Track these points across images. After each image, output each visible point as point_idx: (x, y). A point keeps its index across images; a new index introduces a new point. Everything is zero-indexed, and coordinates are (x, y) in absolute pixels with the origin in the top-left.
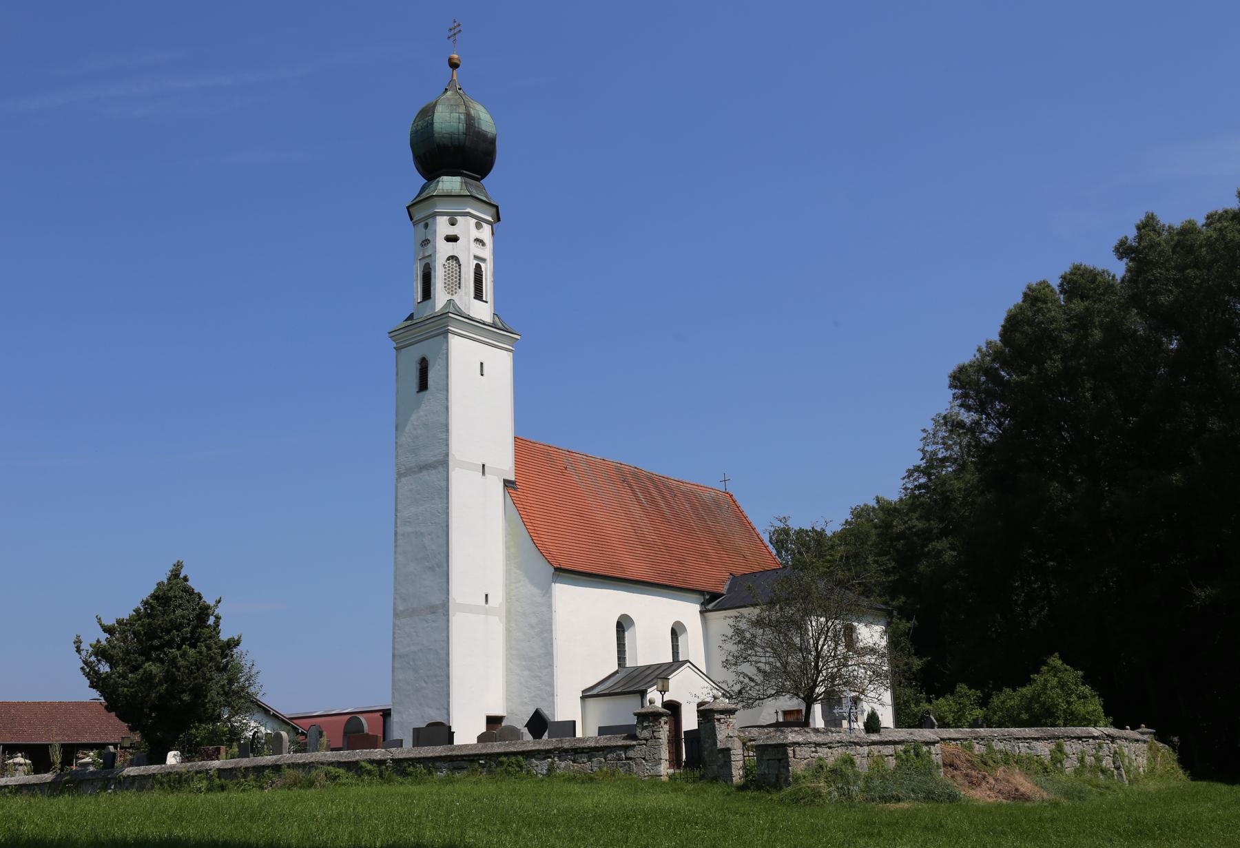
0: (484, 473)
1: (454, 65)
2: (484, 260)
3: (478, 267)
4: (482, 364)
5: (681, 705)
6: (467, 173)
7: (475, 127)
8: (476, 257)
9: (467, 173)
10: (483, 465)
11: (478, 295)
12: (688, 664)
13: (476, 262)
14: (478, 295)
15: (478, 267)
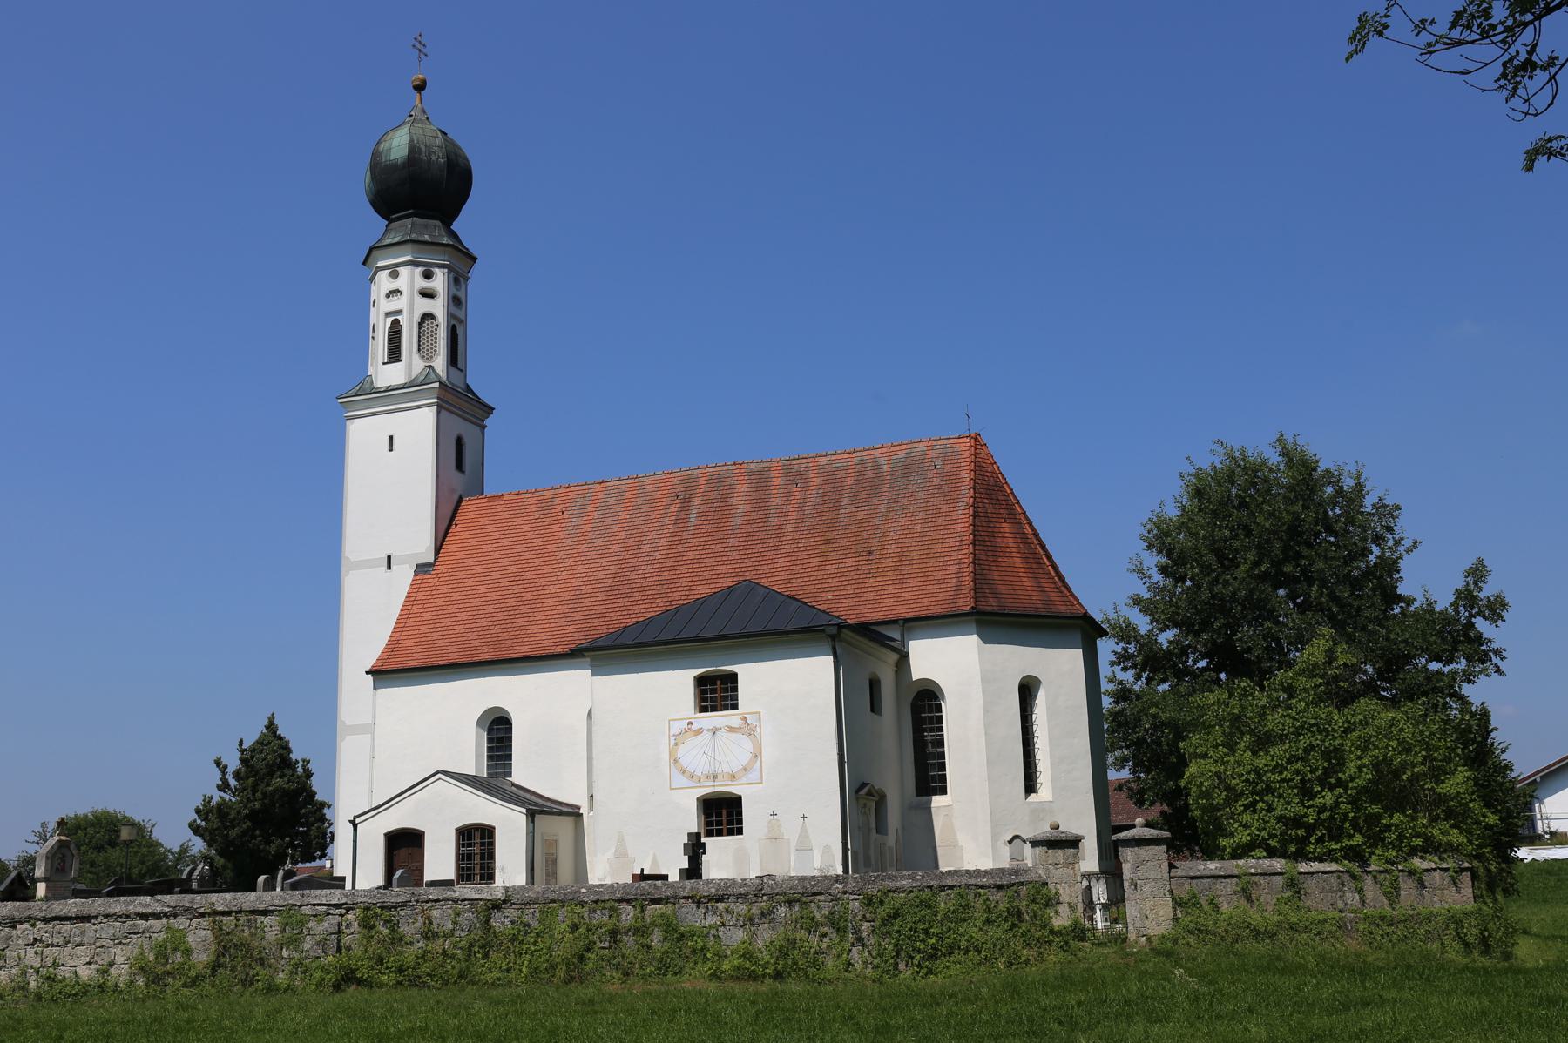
0: (389, 567)
1: (420, 87)
2: (400, 312)
3: (396, 323)
4: (391, 438)
5: (424, 833)
6: (396, 215)
7: (381, 163)
8: (388, 314)
9: (396, 215)
10: (389, 558)
11: (394, 355)
12: (439, 776)
13: (390, 320)
14: (394, 355)
15: (396, 323)
